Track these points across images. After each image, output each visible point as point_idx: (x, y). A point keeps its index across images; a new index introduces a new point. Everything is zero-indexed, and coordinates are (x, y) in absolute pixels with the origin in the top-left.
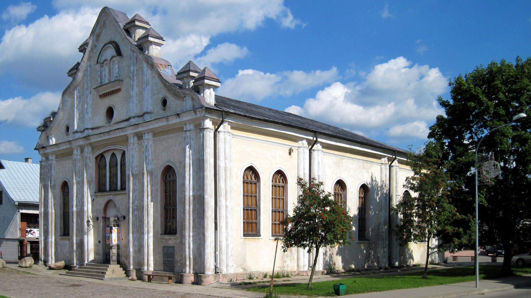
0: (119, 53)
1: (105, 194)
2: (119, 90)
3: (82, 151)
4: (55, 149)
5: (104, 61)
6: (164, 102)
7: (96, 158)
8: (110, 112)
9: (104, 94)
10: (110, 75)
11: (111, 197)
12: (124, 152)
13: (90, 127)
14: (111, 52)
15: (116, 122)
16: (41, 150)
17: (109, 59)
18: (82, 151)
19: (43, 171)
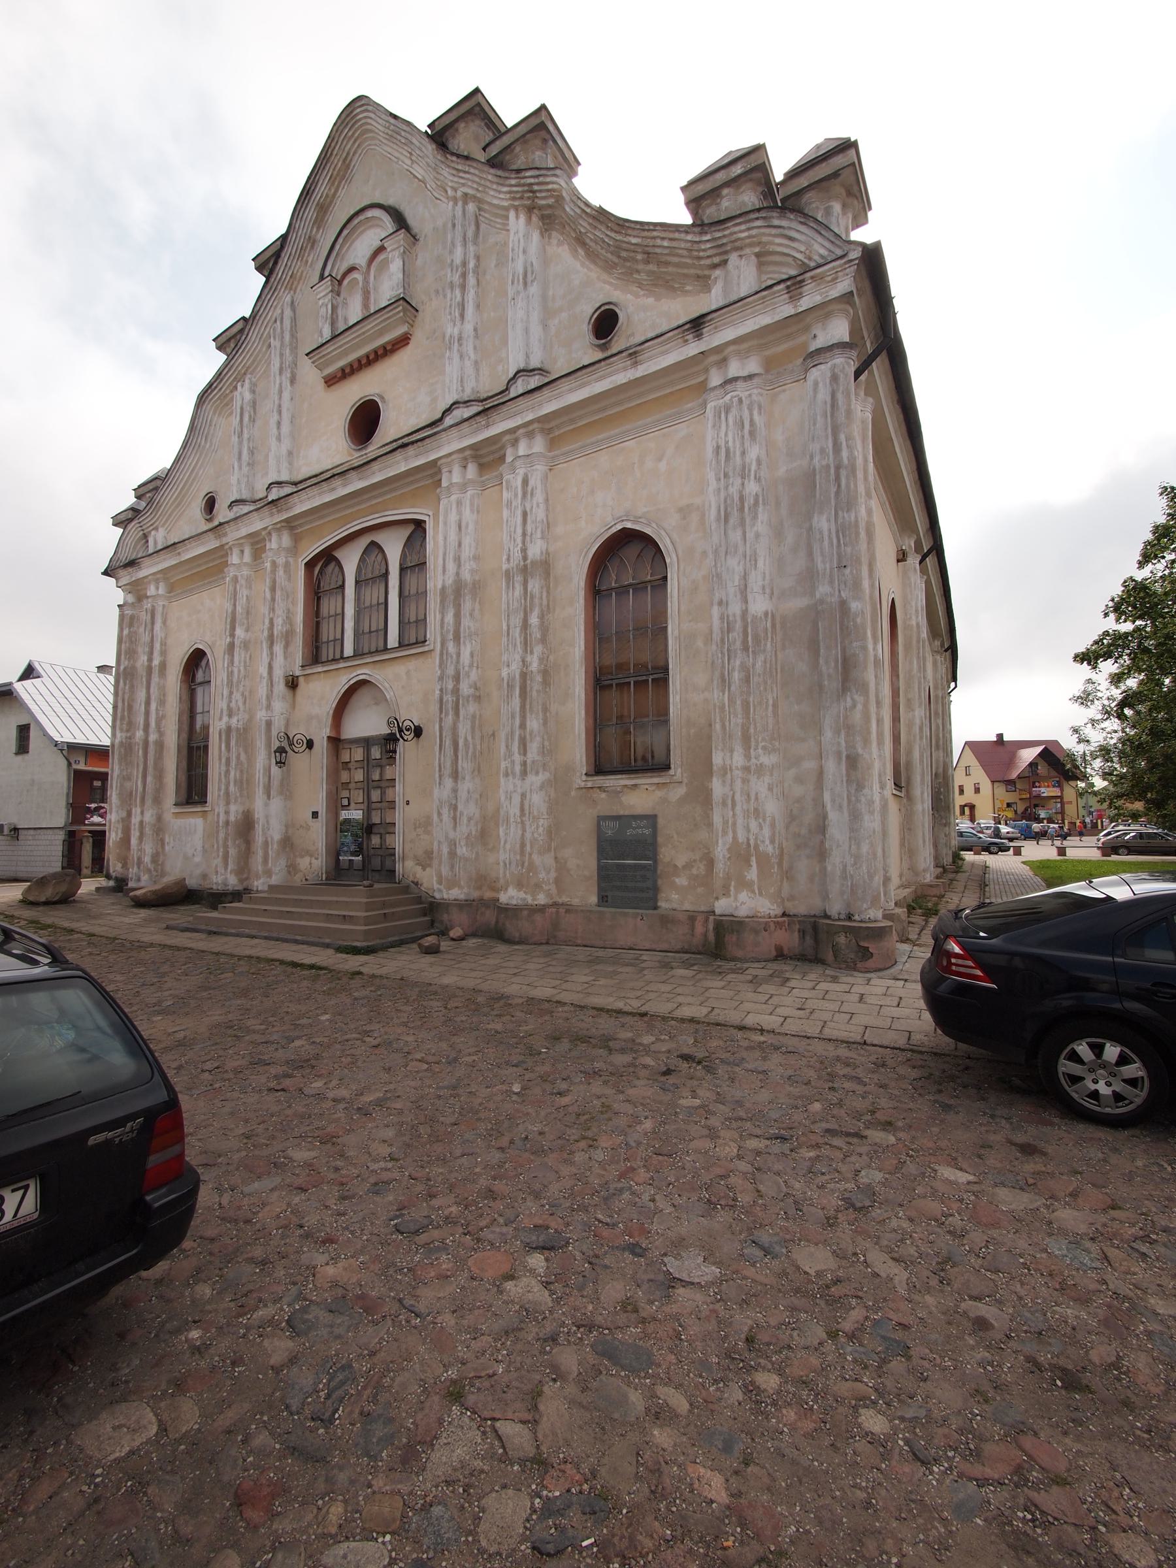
1: (342, 665)
2: (403, 341)
3: (258, 553)
4: (168, 561)
7: (310, 565)
8: (365, 421)
9: (343, 370)
11: (363, 673)
12: (419, 525)
13: (284, 477)
16: (122, 572)
18: (258, 553)
19: (126, 632)
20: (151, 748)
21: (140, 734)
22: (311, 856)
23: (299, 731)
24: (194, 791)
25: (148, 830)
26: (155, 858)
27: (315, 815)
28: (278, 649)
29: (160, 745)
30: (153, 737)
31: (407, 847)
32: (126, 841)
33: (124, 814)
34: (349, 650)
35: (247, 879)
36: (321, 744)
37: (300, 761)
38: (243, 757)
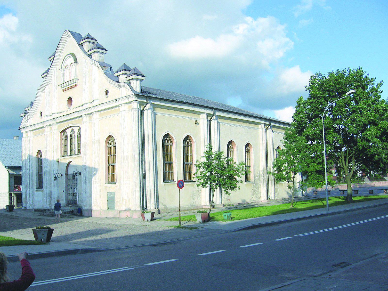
0: (76, 61)
2: (76, 85)
5: (66, 67)
6: (107, 92)
10: (70, 75)
13: (56, 112)
14: (71, 60)
15: (74, 107)
17: (69, 65)
20: (31, 175)
21: (28, 171)
22: (63, 201)
23: (60, 172)
24: (40, 186)
25: (31, 195)
26: (33, 201)
27: (63, 191)
28: (55, 152)
29: (33, 174)
30: (31, 172)
31: (79, 198)
32: (26, 197)
33: (25, 191)
34: (69, 154)
35: (51, 206)
36: (64, 175)
37: (59, 179)
38: (49, 177)
